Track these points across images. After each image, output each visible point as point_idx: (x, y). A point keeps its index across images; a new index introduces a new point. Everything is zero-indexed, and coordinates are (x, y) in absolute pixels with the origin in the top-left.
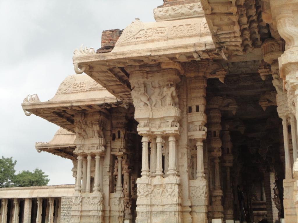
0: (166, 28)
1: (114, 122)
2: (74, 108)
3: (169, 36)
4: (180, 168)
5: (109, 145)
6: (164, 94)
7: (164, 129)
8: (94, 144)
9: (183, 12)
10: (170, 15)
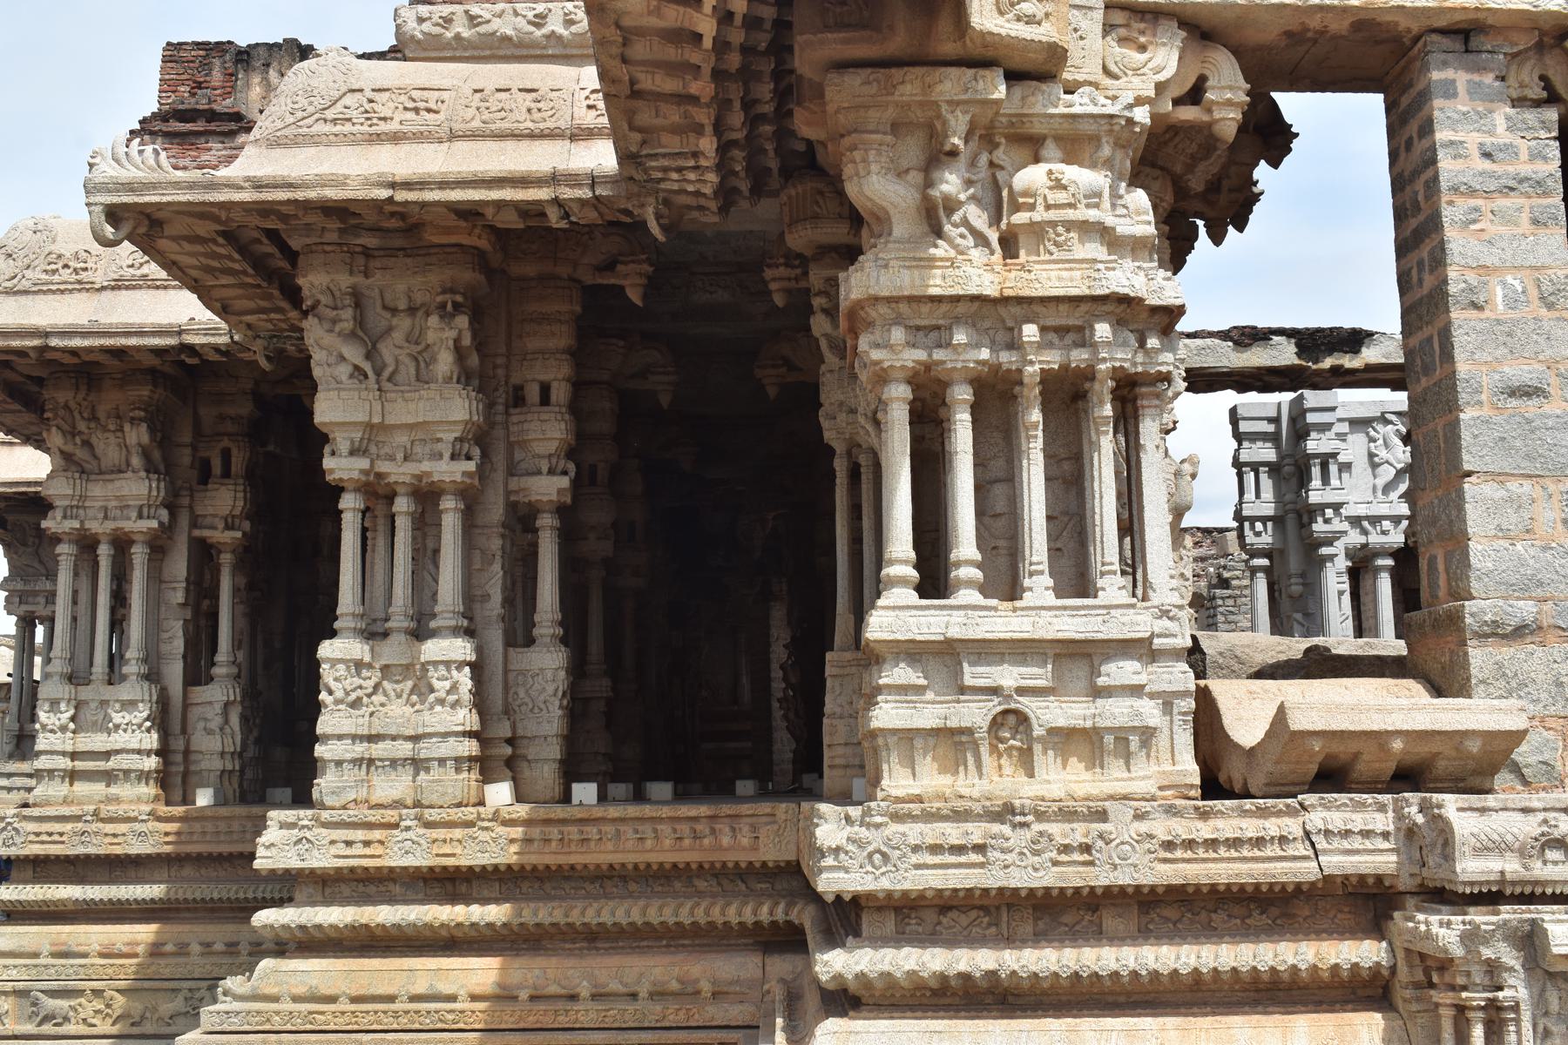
0: (445, 95)
1: (207, 413)
2: (49, 356)
3: (456, 126)
4: (477, 606)
5: (186, 501)
6: (431, 336)
7: (426, 466)
8: (127, 499)
9: (510, 32)
10: (458, 37)
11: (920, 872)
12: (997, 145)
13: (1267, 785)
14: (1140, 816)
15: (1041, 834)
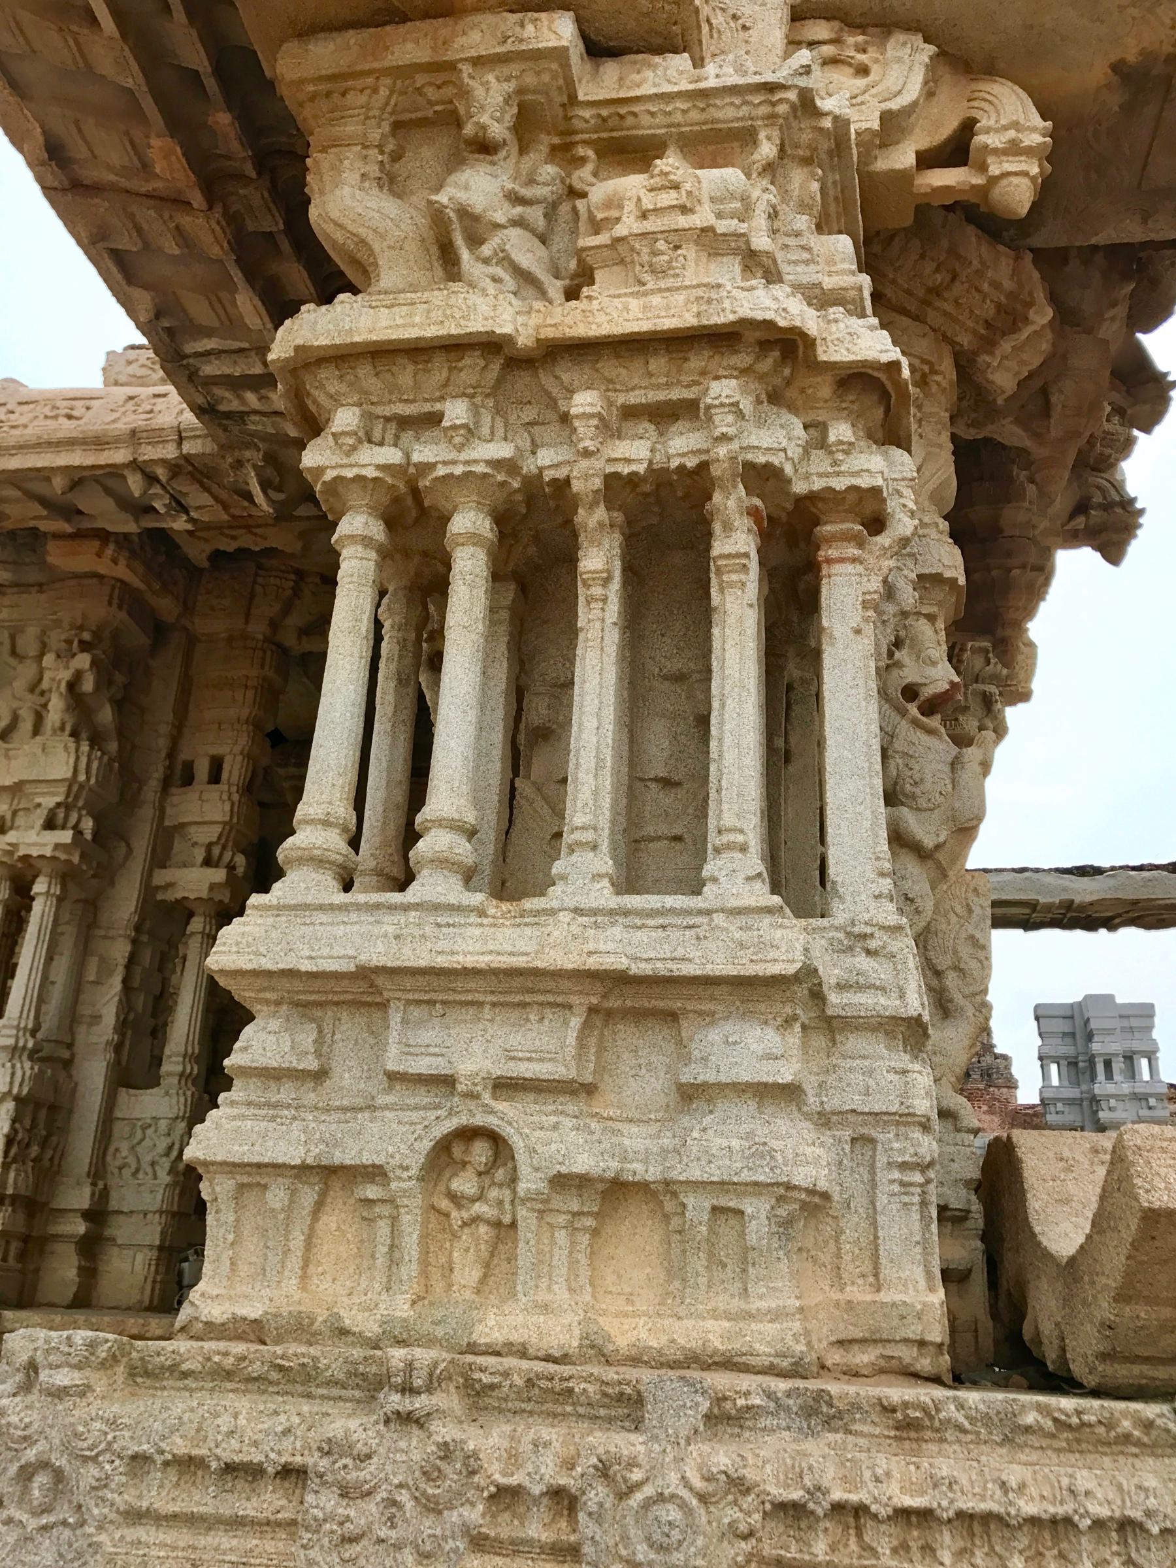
4: (81, 1030)
11: (139, 1533)
12: (583, 160)
13: (1104, 1357)
14: (723, 1418)
15: (446, 1451)
